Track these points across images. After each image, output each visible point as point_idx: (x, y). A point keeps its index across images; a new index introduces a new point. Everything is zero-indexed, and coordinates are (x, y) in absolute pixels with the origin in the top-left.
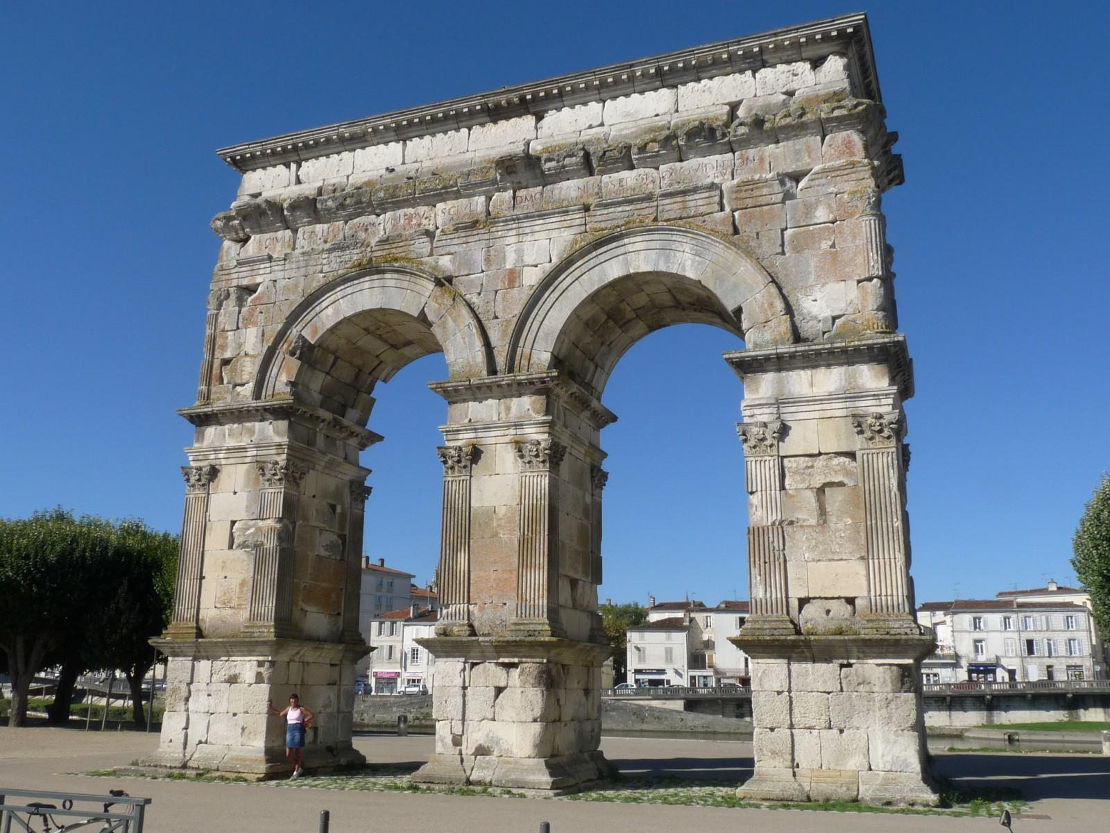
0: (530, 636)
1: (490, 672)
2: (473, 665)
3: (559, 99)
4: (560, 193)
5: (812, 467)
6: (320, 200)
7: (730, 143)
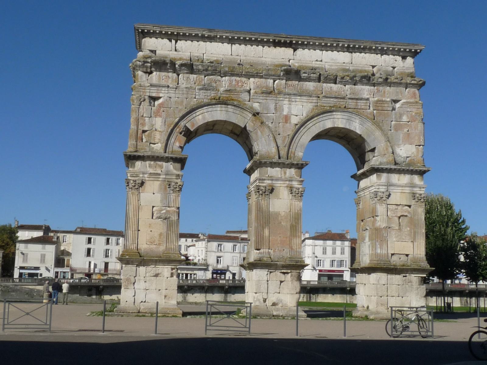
0: (297, 262)
1: (277, 275)
2: (271, 272)
3: (304, 46)
4: (306, 86)
5: (397, 209)
6: (195, 65)
7: (374, 83)
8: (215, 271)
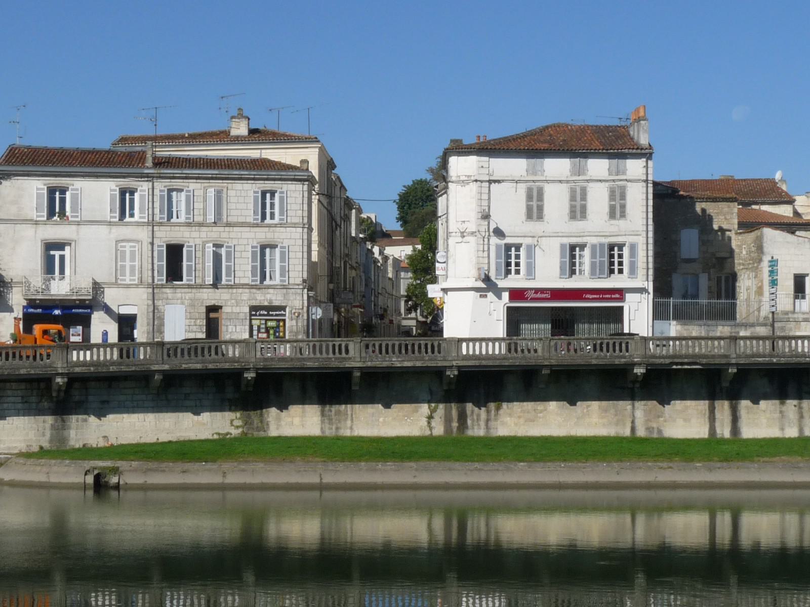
8: (39, 311)
